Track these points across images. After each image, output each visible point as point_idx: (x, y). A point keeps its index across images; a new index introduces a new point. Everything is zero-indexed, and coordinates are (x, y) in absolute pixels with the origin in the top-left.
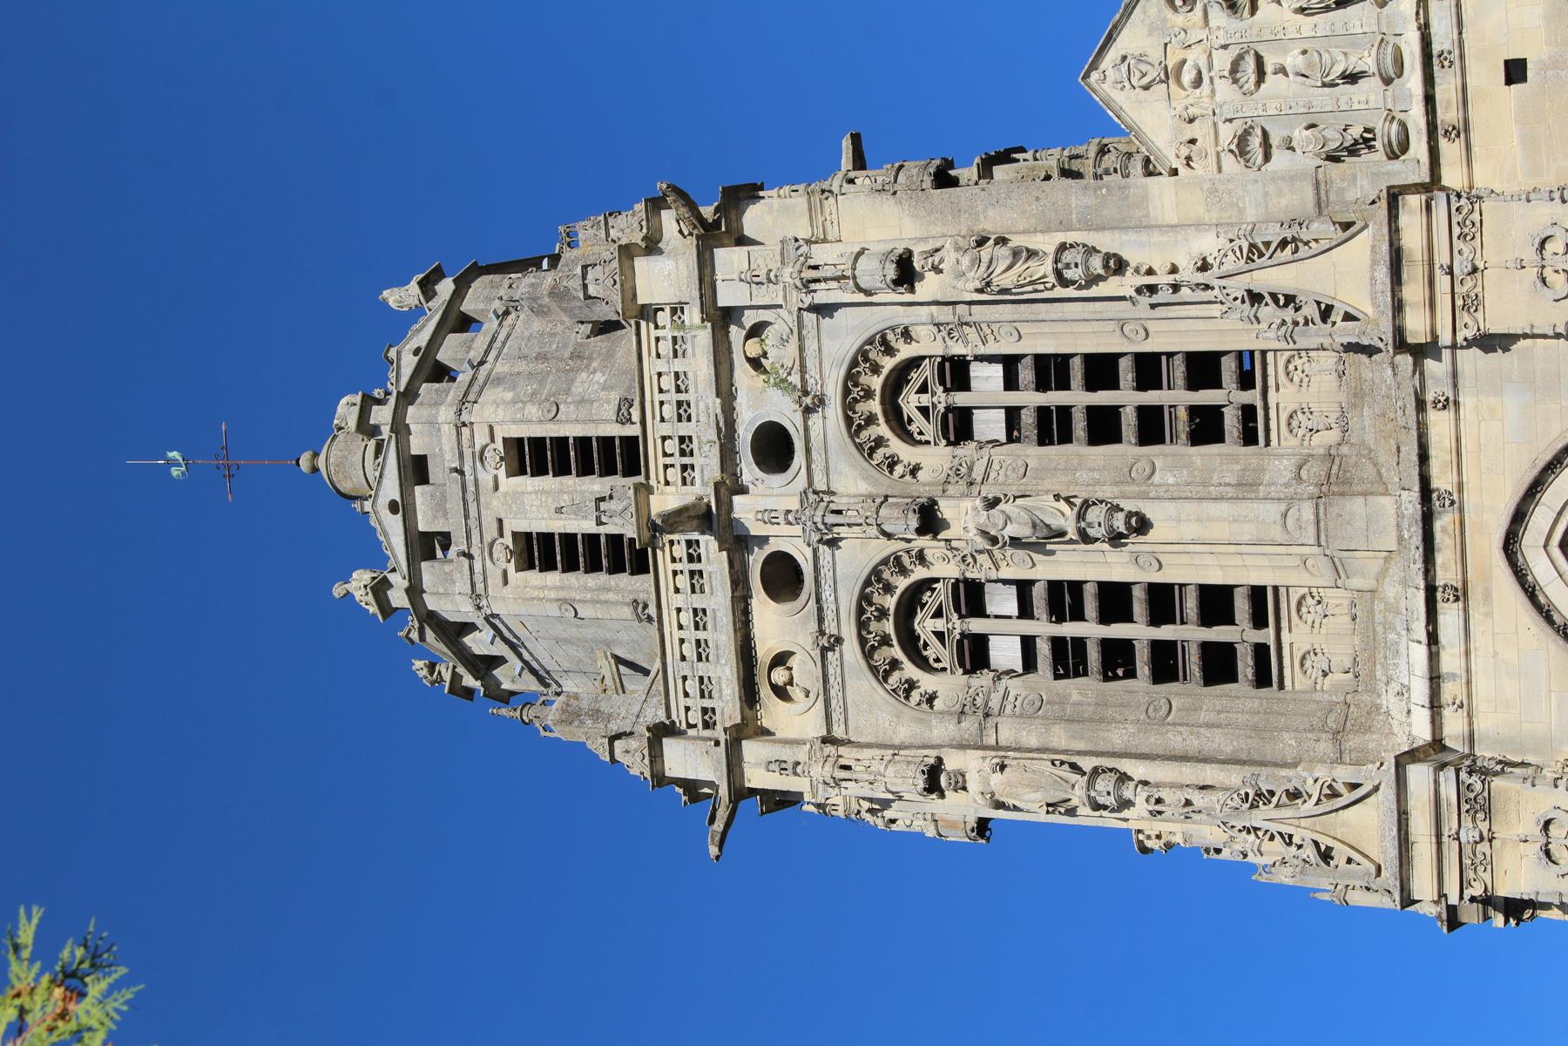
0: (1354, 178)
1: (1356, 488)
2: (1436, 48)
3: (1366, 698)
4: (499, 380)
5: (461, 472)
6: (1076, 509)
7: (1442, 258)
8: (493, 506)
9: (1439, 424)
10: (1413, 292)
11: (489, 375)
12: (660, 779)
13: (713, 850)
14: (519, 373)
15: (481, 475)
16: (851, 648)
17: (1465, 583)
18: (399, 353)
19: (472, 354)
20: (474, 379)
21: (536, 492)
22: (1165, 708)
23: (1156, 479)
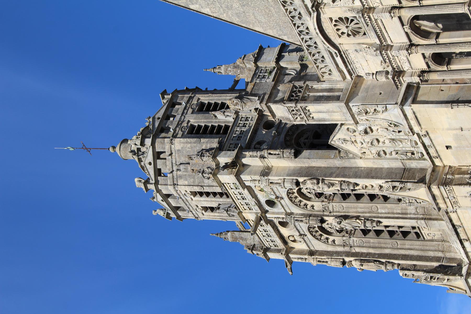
0: (412, 163)
1: (433, 217)
2: (426, 144)
3: (447, 244)
4: (181, 177)
5: (181, 198)
6: (363, 221)
7: (445, 195)
8: (193, 204)
9: (453, 216)
10: (440, 201)
11: (177, 175)
12: (269, 259)
13: (290, 273)
14: (185, 175)
15: (187, 198)
16: (309, 236)
17: (468, 238)
18: (144, 164)
19: (168, 167)
20: (173, 176)
21: (204, 201)
22: (396, 244)
23: (379, 211)
